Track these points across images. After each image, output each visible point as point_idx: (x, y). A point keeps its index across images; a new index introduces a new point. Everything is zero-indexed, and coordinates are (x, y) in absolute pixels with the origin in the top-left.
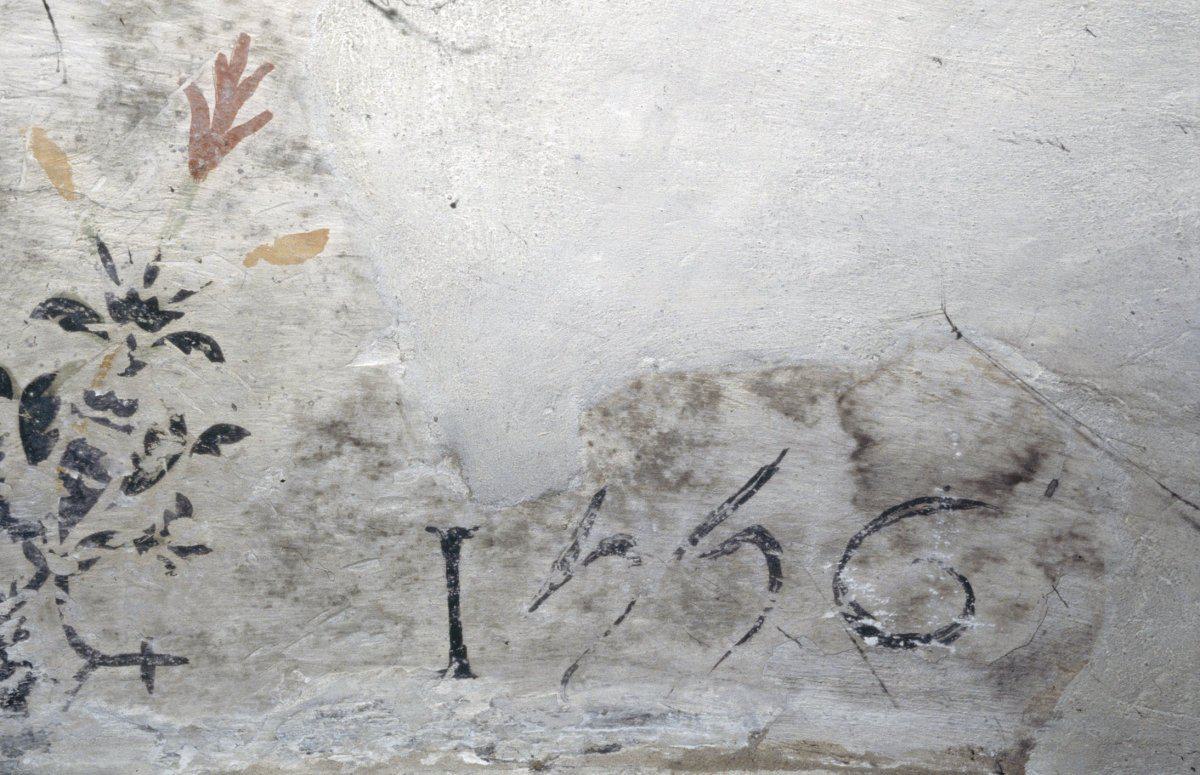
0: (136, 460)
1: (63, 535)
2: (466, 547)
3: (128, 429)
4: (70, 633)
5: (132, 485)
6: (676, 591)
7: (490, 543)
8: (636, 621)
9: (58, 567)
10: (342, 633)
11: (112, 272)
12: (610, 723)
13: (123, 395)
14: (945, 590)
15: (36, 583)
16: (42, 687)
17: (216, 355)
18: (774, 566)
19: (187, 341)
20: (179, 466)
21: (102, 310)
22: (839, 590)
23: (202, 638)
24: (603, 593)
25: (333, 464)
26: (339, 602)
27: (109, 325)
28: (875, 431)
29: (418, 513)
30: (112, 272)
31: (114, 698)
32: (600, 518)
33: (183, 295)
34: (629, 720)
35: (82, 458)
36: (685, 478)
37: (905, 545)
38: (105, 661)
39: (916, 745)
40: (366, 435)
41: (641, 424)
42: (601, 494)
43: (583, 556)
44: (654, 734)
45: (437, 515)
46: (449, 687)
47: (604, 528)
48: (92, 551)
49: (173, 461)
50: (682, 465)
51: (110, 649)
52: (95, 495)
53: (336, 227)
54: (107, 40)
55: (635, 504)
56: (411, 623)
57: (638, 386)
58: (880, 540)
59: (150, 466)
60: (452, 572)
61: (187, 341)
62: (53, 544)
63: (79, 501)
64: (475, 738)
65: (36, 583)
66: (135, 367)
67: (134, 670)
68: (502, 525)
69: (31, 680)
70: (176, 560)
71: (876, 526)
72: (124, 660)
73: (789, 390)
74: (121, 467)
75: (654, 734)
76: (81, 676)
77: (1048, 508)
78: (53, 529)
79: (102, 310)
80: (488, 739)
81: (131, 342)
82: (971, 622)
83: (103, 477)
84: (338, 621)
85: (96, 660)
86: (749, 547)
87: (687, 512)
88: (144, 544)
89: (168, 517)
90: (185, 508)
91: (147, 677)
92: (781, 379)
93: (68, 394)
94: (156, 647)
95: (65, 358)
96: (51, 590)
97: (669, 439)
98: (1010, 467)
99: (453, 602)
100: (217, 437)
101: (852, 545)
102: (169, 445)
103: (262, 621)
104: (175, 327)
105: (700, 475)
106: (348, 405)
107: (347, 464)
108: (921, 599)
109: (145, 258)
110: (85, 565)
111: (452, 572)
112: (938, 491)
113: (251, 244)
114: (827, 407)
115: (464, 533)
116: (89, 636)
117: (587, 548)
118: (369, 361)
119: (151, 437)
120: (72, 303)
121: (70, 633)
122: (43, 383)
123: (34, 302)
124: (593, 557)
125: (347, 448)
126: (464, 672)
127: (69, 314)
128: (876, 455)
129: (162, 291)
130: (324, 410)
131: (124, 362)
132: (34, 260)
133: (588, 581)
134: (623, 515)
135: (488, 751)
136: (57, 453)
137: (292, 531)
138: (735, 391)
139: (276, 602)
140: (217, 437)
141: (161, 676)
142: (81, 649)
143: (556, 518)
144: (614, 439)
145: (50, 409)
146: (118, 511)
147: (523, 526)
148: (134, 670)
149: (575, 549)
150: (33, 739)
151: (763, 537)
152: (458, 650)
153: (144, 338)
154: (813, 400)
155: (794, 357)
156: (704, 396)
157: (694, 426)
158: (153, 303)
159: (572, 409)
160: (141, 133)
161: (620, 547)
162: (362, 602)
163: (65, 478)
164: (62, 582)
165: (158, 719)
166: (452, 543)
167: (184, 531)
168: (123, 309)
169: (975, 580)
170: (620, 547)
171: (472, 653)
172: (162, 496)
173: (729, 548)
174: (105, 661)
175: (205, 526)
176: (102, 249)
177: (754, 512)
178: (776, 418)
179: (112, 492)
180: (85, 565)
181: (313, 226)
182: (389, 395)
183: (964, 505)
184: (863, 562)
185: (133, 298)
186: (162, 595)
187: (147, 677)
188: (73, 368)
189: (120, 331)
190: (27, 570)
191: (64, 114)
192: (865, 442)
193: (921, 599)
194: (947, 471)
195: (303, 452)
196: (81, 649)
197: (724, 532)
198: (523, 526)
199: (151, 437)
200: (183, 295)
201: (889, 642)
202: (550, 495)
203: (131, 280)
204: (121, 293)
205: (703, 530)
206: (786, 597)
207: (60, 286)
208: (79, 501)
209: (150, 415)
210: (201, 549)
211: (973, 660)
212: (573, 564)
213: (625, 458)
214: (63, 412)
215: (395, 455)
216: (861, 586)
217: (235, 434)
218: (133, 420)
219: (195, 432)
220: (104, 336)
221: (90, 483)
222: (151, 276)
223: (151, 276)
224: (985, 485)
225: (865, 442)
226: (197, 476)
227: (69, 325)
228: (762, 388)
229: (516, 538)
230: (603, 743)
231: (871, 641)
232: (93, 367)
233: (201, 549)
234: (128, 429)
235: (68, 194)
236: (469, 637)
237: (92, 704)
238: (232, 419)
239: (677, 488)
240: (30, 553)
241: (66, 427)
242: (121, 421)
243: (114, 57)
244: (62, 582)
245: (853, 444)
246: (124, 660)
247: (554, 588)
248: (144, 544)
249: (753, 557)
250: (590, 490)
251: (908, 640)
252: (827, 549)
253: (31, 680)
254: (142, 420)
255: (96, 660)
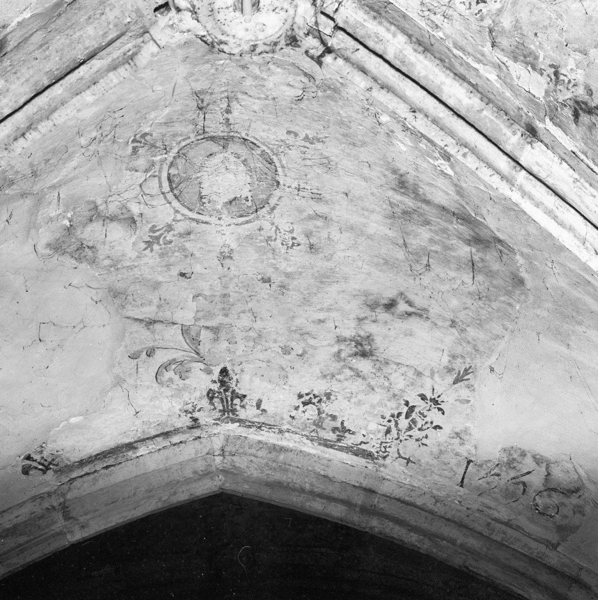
0: (422, 425)
1: (405, 433)
2: (471, 464)
3: (423, 420)
4: (398, 450)
5: (420, 429)
6: (505, 487)
7: (476, 465)
8: (496, 490)
9: (401, 438)
10: (444, 470)
11: (433, 394)
12: (484, 506)
13: (425, 414)
14: (554, 508)
15: (396, 439)
16: (389, 457)
17: (443, 413)
18: (524, 490)
19: (440, 409)
20: (429, 429)
21: (429, 399)
22: (535, 499)
23: (419, 461)
24: (492, 482)
25: (455, 440)
26: (445, 464)
27: (428, 402)
28: (551, 473)
29: (465, 454)
30: (433, 394)
31: (400, 465)
32: (496, 469)
33: (443, 402)
34: (487, 507)
35: (414, 422)
36: (514, 468)
37: (550, 496)
38: (402, 457)
39: (537, 535)
40: (462, 437)
41: (510, 455)
42: (498, 464)
43: (491, 474)
44: (491, 512)
45: (469, 456)
46: (457, 487)
47: (496, 471)
48: (408, 438)
49: (428, 428)
50: (515, 465)
51: (403, 456)
52: (413, 429)
53: (472, 401)
54: (450, 359)
55: (503, 468)
56: (456, 473)
57: (512, 448)
58: (545, 493)
59: (424, 427)
60: (467, 467)
61: (440, 409)
62: (402, 434)
63: (410, 428)
64: (459, 498)
65: (396, 439)
66: (429, 410)
67: (406, 461)
68: (479, 462)
69: (388, 455)
70: (421, 445)
71: (545, 490)
72: (405, 459)
73: (538, 459)
74: (419, 426)
75: (491, 512)
76: (396, 458)
77: (578, 500)
78: (403, 431)
79: (429, 399)
80: (461, 500)
81: (431, 406)
82: (557, 516)
83: (416, 426)
84: (444, 467)
85: (400, 457)
86: (521, 485)
87: (513, 474)
88: (417, 440)
89: (423, 437)
90: (426, 437)
91: (407, 463)
92: (538, 457)
93: (417, 410)
94: (411, 459)
95: (419, 404)
96: (398, 441)
97: (514, 459)
98: (573, 489)
99: (465, 473)
100: (437, 427)
101: (540, 492)
102: (429, 425)
103: (431, 462)
104: (439, 406)
105: (517, 468)
106: (461, 431)
107: (457, 441)
108: (549, 507)
109: (439, 393)
110: (406, 440)
111: (467, 467)
112: (559, 488)
113: (457, 398)
114: (544, 464)
115: (472, 461)
116: (401, 452)
117: (493, 472)
118: (468, 425)
119: (426, 423)
120: (424, 396)
121: (398, 450)
122: (414, 407)
123: (418, 393)
124: (493, 475)
125: (458, 438)
126: (462, 486)
127: (423, 397)
128: (549, 477)
129: (440, 400)
130: (457, 430)
131: (428, 408)
132: (422, 387)
133: (490, 479)
134: (501, 469)
135: (460, 502)
136: (410, 419)
137: (442, 448)
138: (529, 455)
139: (435, 459)
140: (437, 427)
141: (410, 464)
142: (399, 453)
143: (489, 465)
144: (505, 455)
145: (413, 411)
146: (415, 433)
147: (483, 464)
148: (406, 461)
149: (490, 472)
150: (384, 465)
151: (524, 484)
152: (462, 481)
153: (433, 406)
154: (542, 463)
155: (542, 454)
156: (523, 454)
157: (519, 459)
158: (437, 401)
159: (500, 447)
160: (448, 374)
161: (498, 475)
162: (449, 466)
163: (409, 424)
164: (401, 441)
165: (406, 471)
166: (469, 462)
167: (424, 441)
168: (431, 400)
169: (560, 508)
170: (498, 475)
171: (465, 483)
172: (424, 433)
173: (518, 483)
174: (402, 457)
175: (428, 441)
176: (433, 389)
177: (524, 479)
178: (534, 463)
179: (416, 429)
180: (406, 440)
181: (469, 399)
182: (469, 432)
183: (562, 493)
184: (541, 496)
185: (434, 399)
186: (416, 450)
187: (407, 463)
188: (419, 406)
189: (430, 403)
190: (396, 436)
191: (437, 366)
192: (549, 474)
193: (549, 507)
194: (562, 486)
195: (450, 436)
196: (399, 453)
197: (518, 480)
198: (483, 464)
199: (426, 423)
200: (443, 402)
201: (540, 513)
202: (490, 461)
203: (436, 396)
204: (433, 397)
205: (514, 478)
206: (525, 497)
207: (424, 392)
208: (410, 428)
209: (428, 419)
210: (426, 445)
211: (555, 523)
212: (489, 475)
213: (505, 460)
214: (414, 412)
215: (466, 442)
216: (539, 501)
217: (440, 428)
218: (425, 419)
219: (434, 424)
220: (427, 403)
221: (413, 426)
222: (439, 396)
223: (439, 396)
224: (568, 491)
225: (549, 474)
226: (431, 432)
227: (422, 399)
228: (534, 457)
229: (481, 466)
230: (481, 509)
231: (537, 511)
232: (423, 407)
233: (426, 445)
234: (423, 420)
235: (432, 379)
236: (465, 480)
237: (396, 464)
238: (441, 425)
239: (512, 469)
240: (398, 434)
241: (414, 415)
242: (423, 418)
243: (449, 361)
244: (401, 441)
245: (546, 474)
246: (405, 459)
247: (483, 478)
248: (417, 440)
249: (521, 487)
250: (497, 463)
251: (544, 514)
252: (535, 491)
253: (388, 455)
254: (426, 419)
255: (400, 457)
